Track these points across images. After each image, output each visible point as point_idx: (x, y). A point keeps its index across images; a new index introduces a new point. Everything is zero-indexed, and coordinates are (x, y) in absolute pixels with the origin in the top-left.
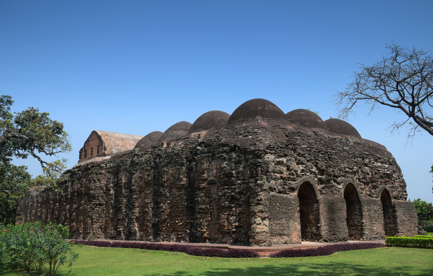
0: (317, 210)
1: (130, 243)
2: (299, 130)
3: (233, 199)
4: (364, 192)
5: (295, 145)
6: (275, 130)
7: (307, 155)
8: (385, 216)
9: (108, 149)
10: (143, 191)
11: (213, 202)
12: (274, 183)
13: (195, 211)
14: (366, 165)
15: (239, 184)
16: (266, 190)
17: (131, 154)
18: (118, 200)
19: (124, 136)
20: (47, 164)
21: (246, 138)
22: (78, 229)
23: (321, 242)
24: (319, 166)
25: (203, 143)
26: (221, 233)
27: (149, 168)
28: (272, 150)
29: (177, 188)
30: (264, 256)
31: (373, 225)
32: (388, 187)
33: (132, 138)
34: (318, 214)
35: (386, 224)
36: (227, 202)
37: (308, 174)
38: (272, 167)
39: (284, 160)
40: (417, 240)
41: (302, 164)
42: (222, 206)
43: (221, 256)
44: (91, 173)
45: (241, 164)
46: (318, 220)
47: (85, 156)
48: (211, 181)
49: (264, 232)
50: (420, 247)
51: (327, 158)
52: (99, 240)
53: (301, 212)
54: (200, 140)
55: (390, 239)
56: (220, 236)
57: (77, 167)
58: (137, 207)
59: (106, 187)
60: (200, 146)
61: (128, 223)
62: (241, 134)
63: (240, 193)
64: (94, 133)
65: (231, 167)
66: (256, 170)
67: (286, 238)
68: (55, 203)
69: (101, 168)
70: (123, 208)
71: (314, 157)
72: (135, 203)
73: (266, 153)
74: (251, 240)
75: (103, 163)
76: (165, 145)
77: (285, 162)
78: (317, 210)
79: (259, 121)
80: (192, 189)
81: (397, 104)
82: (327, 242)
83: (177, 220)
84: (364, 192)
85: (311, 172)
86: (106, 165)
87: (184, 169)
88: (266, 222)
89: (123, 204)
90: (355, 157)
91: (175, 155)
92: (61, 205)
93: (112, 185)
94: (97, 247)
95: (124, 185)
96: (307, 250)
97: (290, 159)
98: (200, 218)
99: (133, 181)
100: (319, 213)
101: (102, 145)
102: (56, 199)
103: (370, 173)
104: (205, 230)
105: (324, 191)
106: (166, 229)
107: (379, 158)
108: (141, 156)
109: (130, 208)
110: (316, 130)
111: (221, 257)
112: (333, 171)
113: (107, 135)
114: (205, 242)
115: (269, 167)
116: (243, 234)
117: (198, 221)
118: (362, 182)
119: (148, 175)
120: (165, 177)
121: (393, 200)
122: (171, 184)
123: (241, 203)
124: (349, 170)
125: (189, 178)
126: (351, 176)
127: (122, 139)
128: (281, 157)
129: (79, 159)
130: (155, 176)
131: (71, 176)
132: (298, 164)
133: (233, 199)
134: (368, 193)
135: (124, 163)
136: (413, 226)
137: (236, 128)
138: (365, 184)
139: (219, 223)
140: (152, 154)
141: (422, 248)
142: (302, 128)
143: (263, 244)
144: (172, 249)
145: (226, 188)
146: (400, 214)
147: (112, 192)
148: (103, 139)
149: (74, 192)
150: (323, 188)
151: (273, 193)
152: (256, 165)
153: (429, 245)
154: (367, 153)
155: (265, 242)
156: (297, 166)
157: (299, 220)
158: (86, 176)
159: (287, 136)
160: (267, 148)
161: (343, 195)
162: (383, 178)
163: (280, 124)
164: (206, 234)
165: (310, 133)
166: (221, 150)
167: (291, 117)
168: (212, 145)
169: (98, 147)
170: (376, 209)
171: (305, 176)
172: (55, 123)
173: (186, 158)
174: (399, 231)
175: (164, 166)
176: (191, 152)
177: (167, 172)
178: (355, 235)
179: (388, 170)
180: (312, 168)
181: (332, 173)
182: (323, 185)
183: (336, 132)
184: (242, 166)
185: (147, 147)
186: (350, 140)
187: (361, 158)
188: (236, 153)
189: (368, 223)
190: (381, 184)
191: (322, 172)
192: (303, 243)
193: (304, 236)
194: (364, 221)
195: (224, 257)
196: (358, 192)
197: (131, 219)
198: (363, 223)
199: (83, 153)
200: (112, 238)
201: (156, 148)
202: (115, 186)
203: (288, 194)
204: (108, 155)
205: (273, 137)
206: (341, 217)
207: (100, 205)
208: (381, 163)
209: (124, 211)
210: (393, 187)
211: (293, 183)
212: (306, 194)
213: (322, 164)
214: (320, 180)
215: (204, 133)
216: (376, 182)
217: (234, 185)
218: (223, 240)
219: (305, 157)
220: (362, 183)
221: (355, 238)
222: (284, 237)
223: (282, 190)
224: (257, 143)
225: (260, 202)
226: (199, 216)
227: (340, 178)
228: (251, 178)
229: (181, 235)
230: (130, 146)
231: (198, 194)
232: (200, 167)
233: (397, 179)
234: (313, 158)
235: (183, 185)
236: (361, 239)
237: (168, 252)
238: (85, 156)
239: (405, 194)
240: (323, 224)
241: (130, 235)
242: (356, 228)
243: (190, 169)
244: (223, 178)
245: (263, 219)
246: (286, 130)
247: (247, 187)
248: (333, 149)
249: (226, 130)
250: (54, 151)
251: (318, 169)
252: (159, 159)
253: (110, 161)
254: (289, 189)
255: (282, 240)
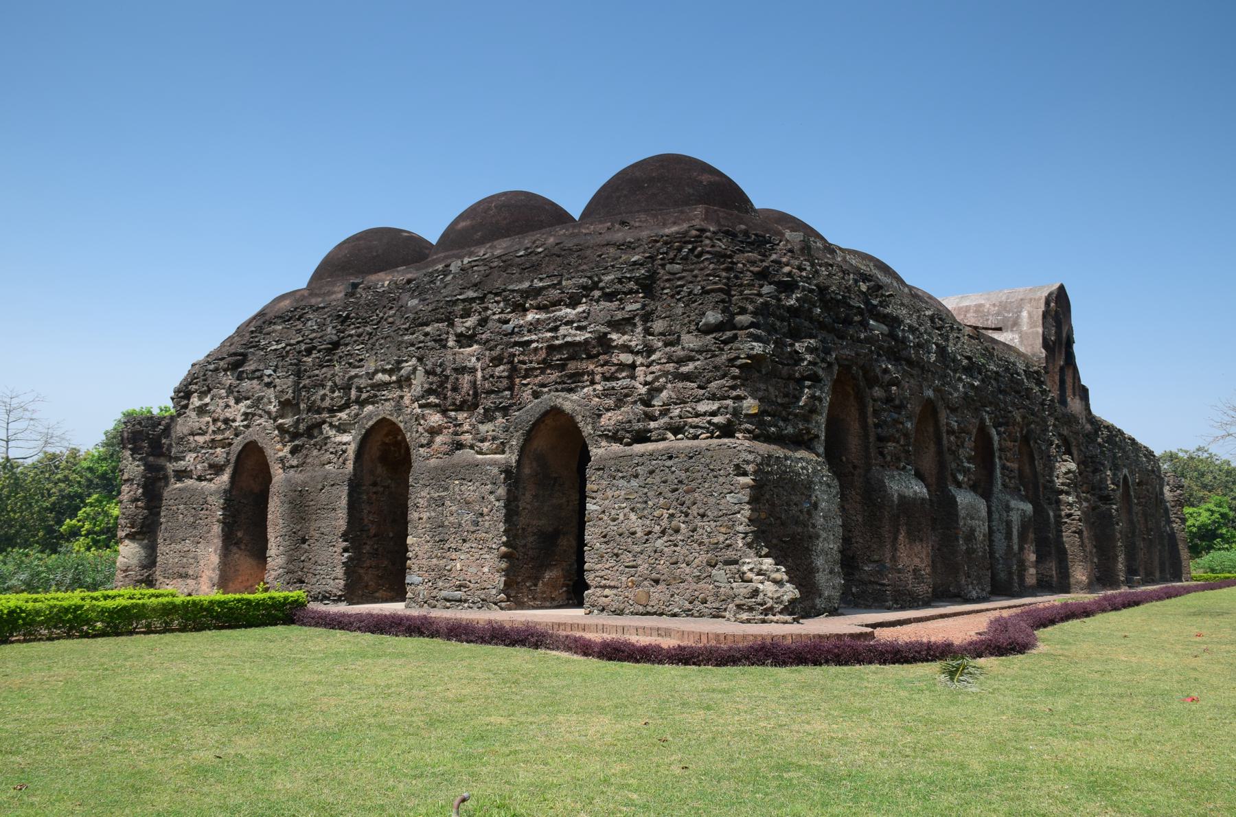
124: (386, 378)
179: (578, 328)
190: (536, 395)
206: (326, 531)
208: (539, 308)
222: (189, 581)
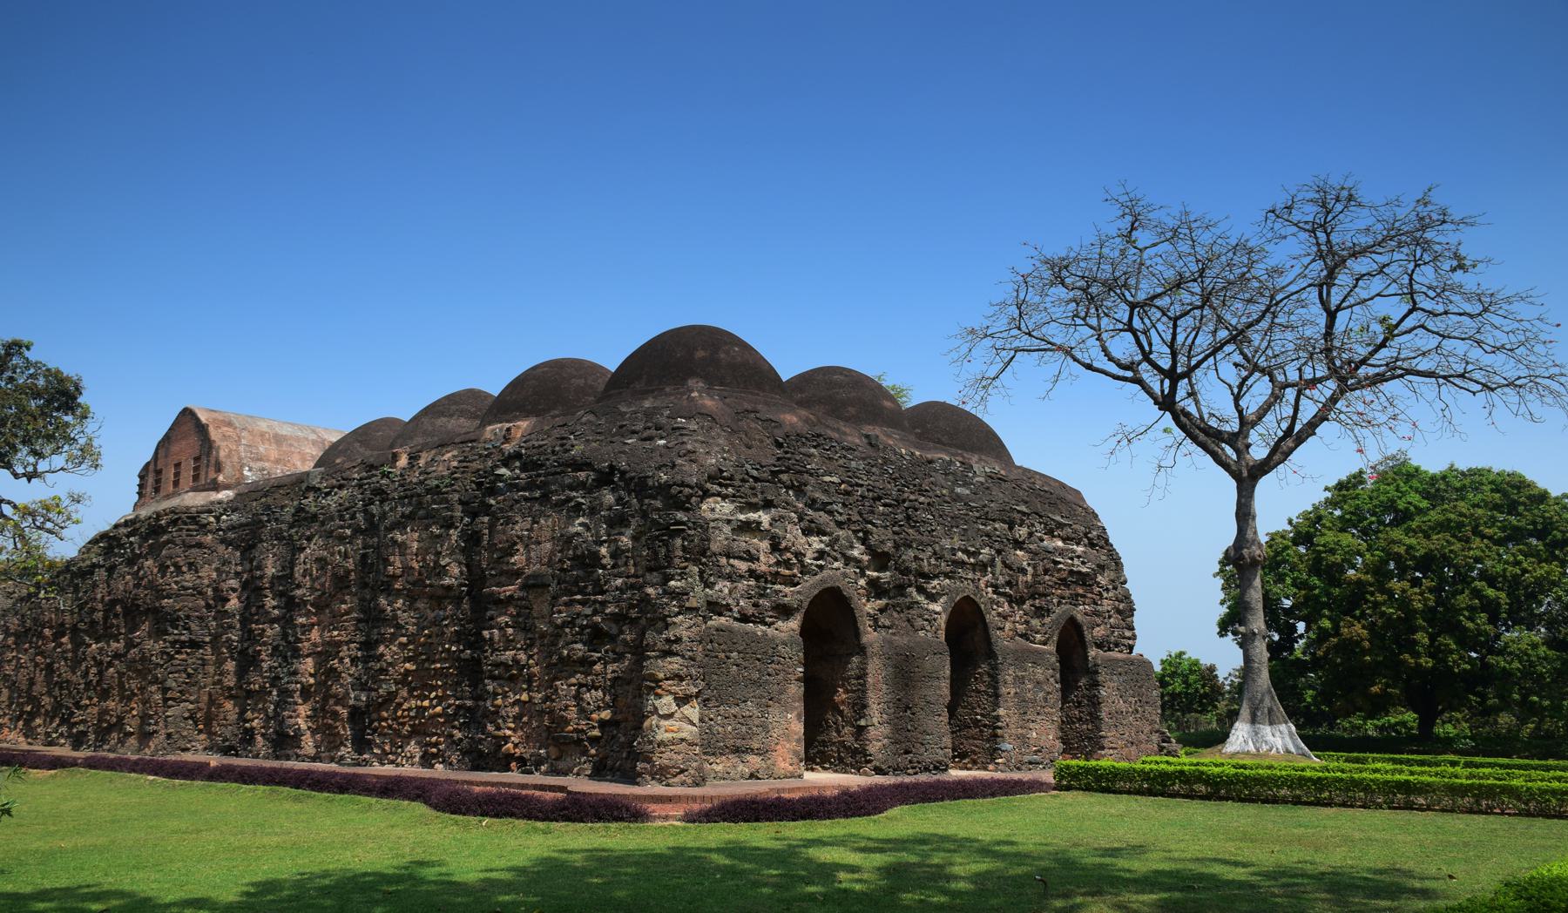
0: (858, 678)
1: (288, 771)
2: (818, 430)
3: (596, 637)
4: (1008, 625)
5: (800, 473)
6: (743, 424)
7: (839, 507)
8: (1064, 699)
9: (228, 470)
10: (328, 606)
11: (538, 643)
12: (726, 591)
13: (482, 672)
14: (1018, 544)
15: (617, 588)
16: (697, 609)
17: (299, 485)
18: (251, 631)
19: (285, 431)
20: (15, 507)
21: (647, 445)
22: (120, 719)
23: (866, 774)
24: (873, 540)
25: (518, 456)
26: (558, 745)
27: (348, 532)
28: (727, 486)
29: (431, 597)
30: (666, 818)
31: (1031, 726)
32: (1080, 612)
33: (314, 437)
34: (863, 690)
35: (1066, 724)
36: (579, 646)
37: (836, 564)
38: (721, 538)
39: (764, 518)
40: (1142, 770)
41: (821, 532)
42: (561, 658)
43: (529, 816)
44: (168, 542)
45: (628, 526)
46: (860, 707)
47: (157, 490)
48: (534, 576)
49: (683, 740)
50: (1150, 793)
51: (899, 517)
52: (188, 757)
53: (809, 680)
54: (509, 448)
55: (1068, 767)
56: (554, 751)
57: (126, 524)
58: (308, 656)
59: (216, 590)
60: (506, 464)
61: (277, 705)
62: (634, 432)
63: (618, 618)
64: (187, 414)
65: (598, 535)
66: (666, 544)
67: (754, 760)
68: (58, 636)
69: (204, 527)
70: (263, 656)
71: (860, 514)
72: (300, 641)
73: (706, 494)
74: (640, 766)
75: (210, 512)
76: (403, 462)
77: (765, 525)
78: (858, 678)
79: (695, 394)
80: (478, 598)
81: (1129, 373)
82: (885, 774)
83: (426, 697)
84: (1008, 625)
85: (848, 560)
86: (218, 518)
87: (454, 538)
88: (693, 711)
89: (265, 644)
90: (987, 519)
91: (428, 491)
92: (78, 644)
93: (234, 583)
94: (160, 779)
95: (272, 583)
96: (803, 801)
97: (782, 517)
98: (496, 694)
99: (298, 570)
100: (864, 685)
101: (209, 454)
102: (62, 624)
103: (1030, 569)
104: (508, 733)
105: (884, 621)
106: (390, 727)
107: (1060, 526)
108: (327, 494)
109: (285, 658)
110: (874, 430)
111: (530, 819)
112: (916, 558)
113: (230, 424)
114: (509, 770)
115: (709, 540)
116: (622, 746)
117: (488, 703)
118: (1004, 595)
119: (346, 556)
120: (397, 561)
121: (1093, 652)
122: (414, 584)
123: (619, 649)
124: (965, 557)
125: (467, 566)
126: (970, 576)
127: (278, 440)
128: (754, 507)
129: (136, 497)
130: (364, 556)
131: (108, 552)
132: (807, 532)
133: (596, 637)
134: (1021, 628)
135: (276, 512)
136: (1147, 729)
137: (623, 414)
138: (1011, 600)
139: (551, 712)
140: (360, 486)
141: (1155, 795)
142: (831, 422)
143: (676, 780)
144: (390, 789)
145: (579, 602)
146: (1109, 691)
147: (234, 604)
148: (214, 434)
149: (114, 602)
150: (882, 611)
151: (723, 620)
152: (670, 531)
153: (1176, 787)
154: (1023, 508)
155: (682, 771)
156: (803, 540)
157: (800, 706)
158: (154, 551)
159: (779, 445)
160: (711, 478)
161: (942, 634)
162: (1068, 586)
163: (759, 407)
164: (510, 745)
165: (854, 439)
166: (568, 481)
167: (801, 391)
168: (542, 465)
169: (197, 459)
170: (1041, 677)
171: (825, 573)
172: (56, 377)
173: (461, 502)
174: (1106, 743)
175: (390, 529)
176: (479, 485)
177: (403, 546)
178: (974, 752)
180: (852, 547)
181: (914, 565)
182: (882, 602)
183: (940, 442)
184: (629, 532)
185: (347, 466)
186: (976, 467)
187: (1004, 522)
188: (613, 491)
189: (1014, 719)
190: (1059, 603)
191: (881, 560)
192: (809, 776)
193: (815, 753)
194: (1001, 712)
195: (537, 819)
196: (991, 626)
197: (285, 693)
198: (998, 718)
199: (151, 480)
200: (226, 751)
201: (376, 468)
202: (245, 585)
203: (770, 625)
204: (227, 487)
205: (732, 444)
207: (195, 645)
208: (1064, 540)
209: (265, 665)
210: (1096, 613)
211: (788, 590)
212: (829, 629)
213: (883, 537)
214: (873, 583)
215: (523, 425)
216: (1046, 595)
217: (602, 593)
218: (561, 765)
219: (830, 513)
220: (1002, 599)
221: (974, 762)
222: (750, 757)
223: (751, 611)
224: (679, 461)
225: (675, 647)
226: (490, 688)
227: (935, 582)
228: (650, 570)
229: (436, 745)
230: (304, 460)
231: (492, 618)
232: (504, 532)
233: (1107, 590)
234: (856, 517)
235: (449, 588)
236: (991, 767)
237: (373, 800)
238: (157, 490)
239: (1128, 634)
240: (875, 720)
241: (284, 742)
242: (976, 734)
243: (472, 539)
244: (572, 568)
245: (682, 700)
246: (779, 425)
247: (641, 601)
248: (922, 492)
249: (591, 417)
250: (43, 466)
251: (870, 550)
252: (382, 502)
253: (231, 507)
254: (773, 609)
255: (741, 767)
